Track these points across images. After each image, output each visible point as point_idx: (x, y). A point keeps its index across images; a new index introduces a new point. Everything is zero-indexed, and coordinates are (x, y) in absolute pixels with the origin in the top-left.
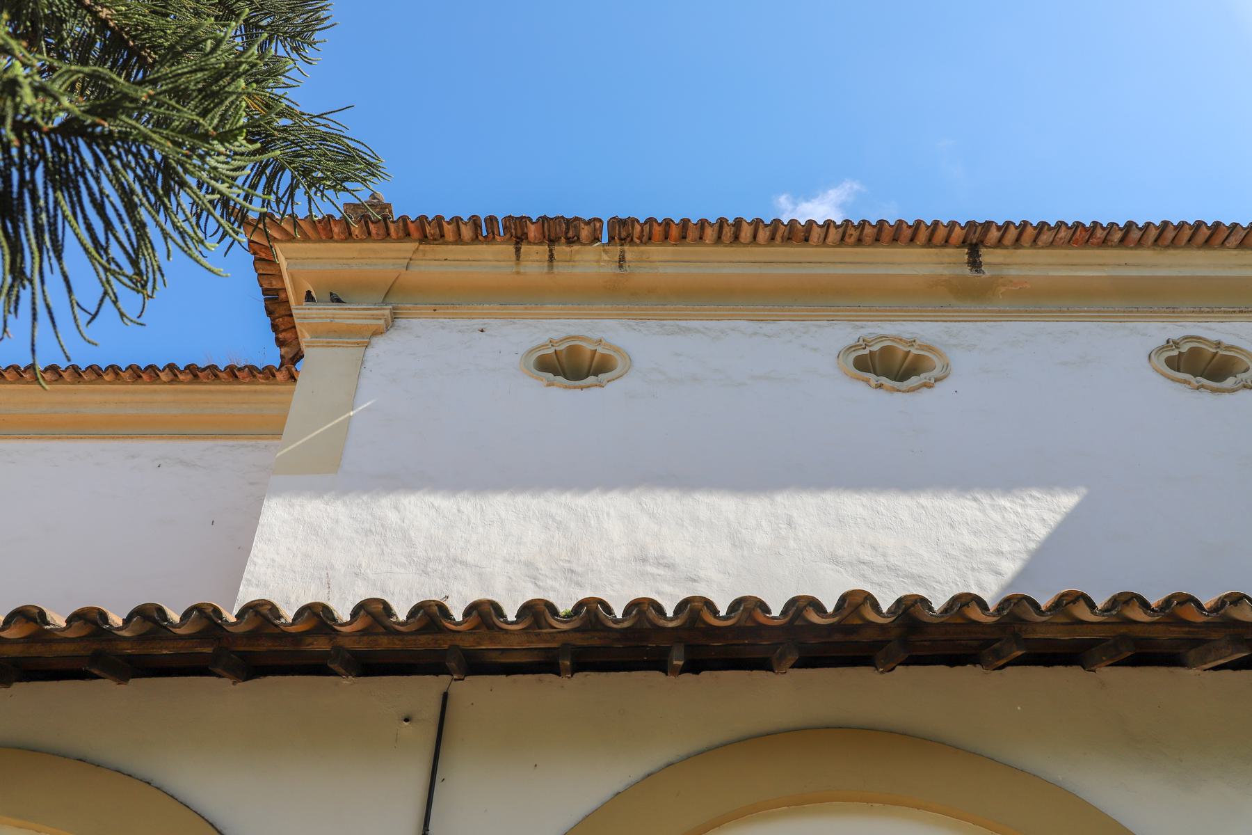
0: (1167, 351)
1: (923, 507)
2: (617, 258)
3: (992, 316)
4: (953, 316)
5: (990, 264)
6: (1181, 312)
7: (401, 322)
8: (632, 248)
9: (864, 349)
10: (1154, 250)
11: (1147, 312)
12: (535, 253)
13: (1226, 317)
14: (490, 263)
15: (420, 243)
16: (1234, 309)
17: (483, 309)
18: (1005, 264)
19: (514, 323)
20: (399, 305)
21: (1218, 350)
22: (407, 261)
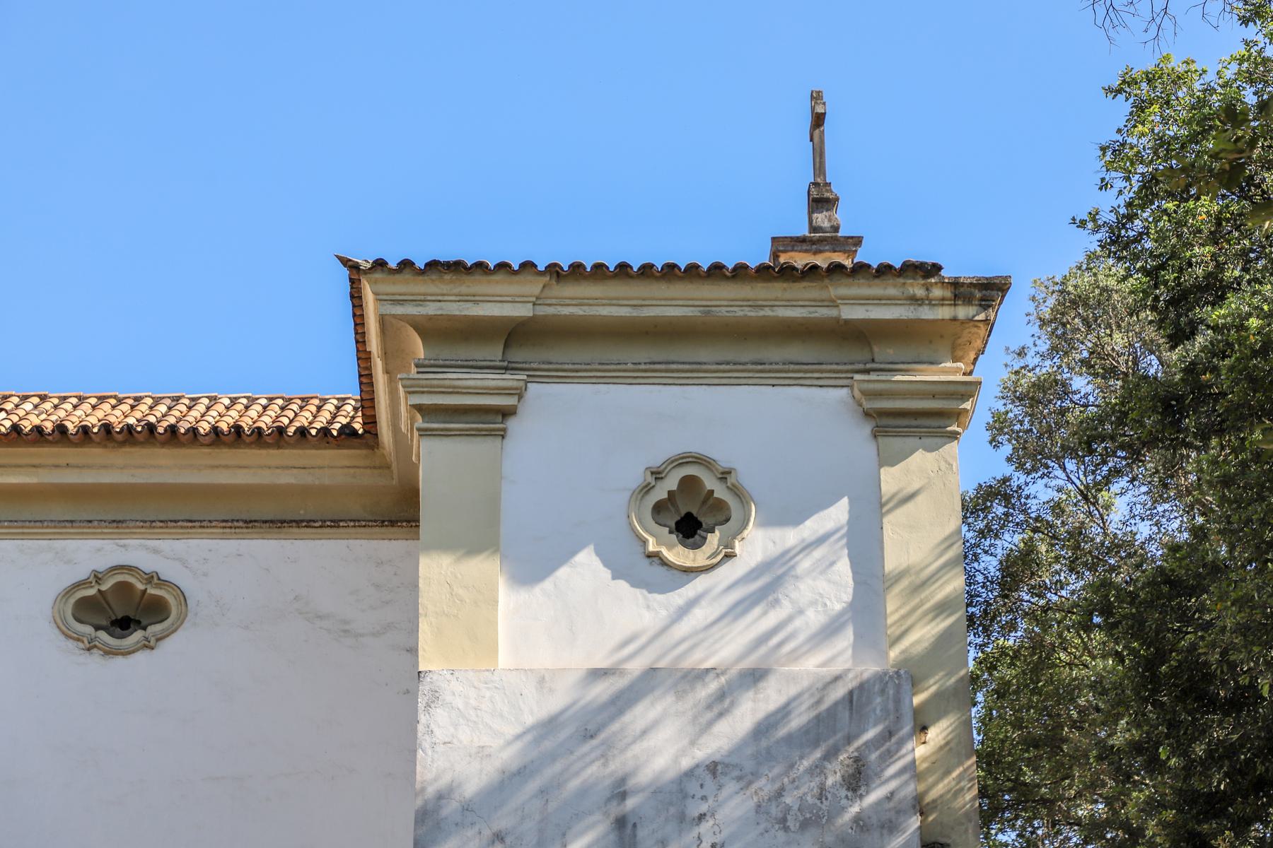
0: (84, 588)
6: (128, 527)
10: (105, 446)
11: (84, 527)
21: (148, 586)
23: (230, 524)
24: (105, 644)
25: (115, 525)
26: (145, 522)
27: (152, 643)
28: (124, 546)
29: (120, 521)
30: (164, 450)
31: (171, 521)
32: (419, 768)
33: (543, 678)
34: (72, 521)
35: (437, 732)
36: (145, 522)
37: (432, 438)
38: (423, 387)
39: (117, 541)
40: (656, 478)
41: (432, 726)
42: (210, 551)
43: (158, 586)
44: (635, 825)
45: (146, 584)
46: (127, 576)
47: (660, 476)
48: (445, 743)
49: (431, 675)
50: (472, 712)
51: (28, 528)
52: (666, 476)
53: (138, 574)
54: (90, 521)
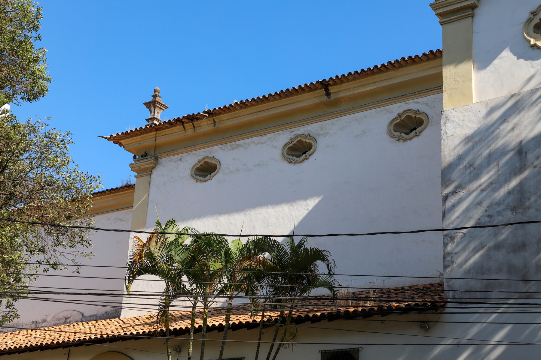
0: (396, 120)
1: (292, 215)
2: (213, 122)
3: (337, 115)
4: (324, 119)
5: (333, 93)
6: (407, 97)
7: (160, 161)
8: (216, 117)
9: (291, 143)
10: (394, 70)
12: (189, 125)
13: (425, 94)
14: (178, 133)
15: (156, 131)
16: (428, 90)
17: (180, 151)
18: (339, 92)
19: (190, 154)
20: (158, 155)
22: (155, 138)
23: (440, 88)
24: (404, 137)
25: (403, 97)
26: (412, 93)
27: (418, 134)
28: (407, 103)
29: (404, 95)
30: (412, 67)
31: (420, 91)
32: (442, 147)
33: (488, 103)
34: (390, 99)
35: (448, 132)
36: (412, 93)
37: (446, 25)
38: (439, 6)
39: (405, 102)
40: (534, 15)
41: (447, 130)
42: (435, 98)
43: (419, 114)
44: (526, 153)
45: (415, 114)
46: (409, 113)
47: (535, 14)
48: (451, 136)
49: (445, 112)
50: (461, 122)
51: (377, 104)
52: (538, 13)
53: (412, 111)
54: (395, 97)
